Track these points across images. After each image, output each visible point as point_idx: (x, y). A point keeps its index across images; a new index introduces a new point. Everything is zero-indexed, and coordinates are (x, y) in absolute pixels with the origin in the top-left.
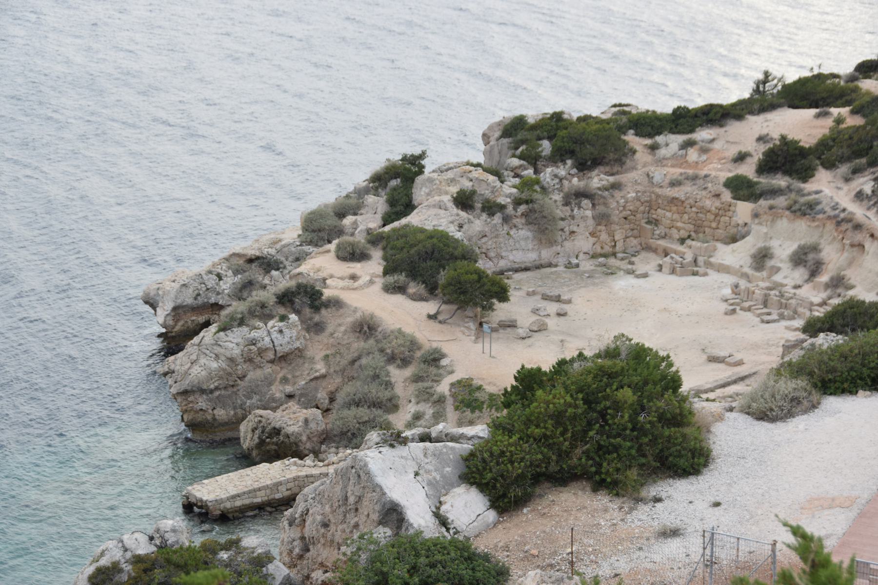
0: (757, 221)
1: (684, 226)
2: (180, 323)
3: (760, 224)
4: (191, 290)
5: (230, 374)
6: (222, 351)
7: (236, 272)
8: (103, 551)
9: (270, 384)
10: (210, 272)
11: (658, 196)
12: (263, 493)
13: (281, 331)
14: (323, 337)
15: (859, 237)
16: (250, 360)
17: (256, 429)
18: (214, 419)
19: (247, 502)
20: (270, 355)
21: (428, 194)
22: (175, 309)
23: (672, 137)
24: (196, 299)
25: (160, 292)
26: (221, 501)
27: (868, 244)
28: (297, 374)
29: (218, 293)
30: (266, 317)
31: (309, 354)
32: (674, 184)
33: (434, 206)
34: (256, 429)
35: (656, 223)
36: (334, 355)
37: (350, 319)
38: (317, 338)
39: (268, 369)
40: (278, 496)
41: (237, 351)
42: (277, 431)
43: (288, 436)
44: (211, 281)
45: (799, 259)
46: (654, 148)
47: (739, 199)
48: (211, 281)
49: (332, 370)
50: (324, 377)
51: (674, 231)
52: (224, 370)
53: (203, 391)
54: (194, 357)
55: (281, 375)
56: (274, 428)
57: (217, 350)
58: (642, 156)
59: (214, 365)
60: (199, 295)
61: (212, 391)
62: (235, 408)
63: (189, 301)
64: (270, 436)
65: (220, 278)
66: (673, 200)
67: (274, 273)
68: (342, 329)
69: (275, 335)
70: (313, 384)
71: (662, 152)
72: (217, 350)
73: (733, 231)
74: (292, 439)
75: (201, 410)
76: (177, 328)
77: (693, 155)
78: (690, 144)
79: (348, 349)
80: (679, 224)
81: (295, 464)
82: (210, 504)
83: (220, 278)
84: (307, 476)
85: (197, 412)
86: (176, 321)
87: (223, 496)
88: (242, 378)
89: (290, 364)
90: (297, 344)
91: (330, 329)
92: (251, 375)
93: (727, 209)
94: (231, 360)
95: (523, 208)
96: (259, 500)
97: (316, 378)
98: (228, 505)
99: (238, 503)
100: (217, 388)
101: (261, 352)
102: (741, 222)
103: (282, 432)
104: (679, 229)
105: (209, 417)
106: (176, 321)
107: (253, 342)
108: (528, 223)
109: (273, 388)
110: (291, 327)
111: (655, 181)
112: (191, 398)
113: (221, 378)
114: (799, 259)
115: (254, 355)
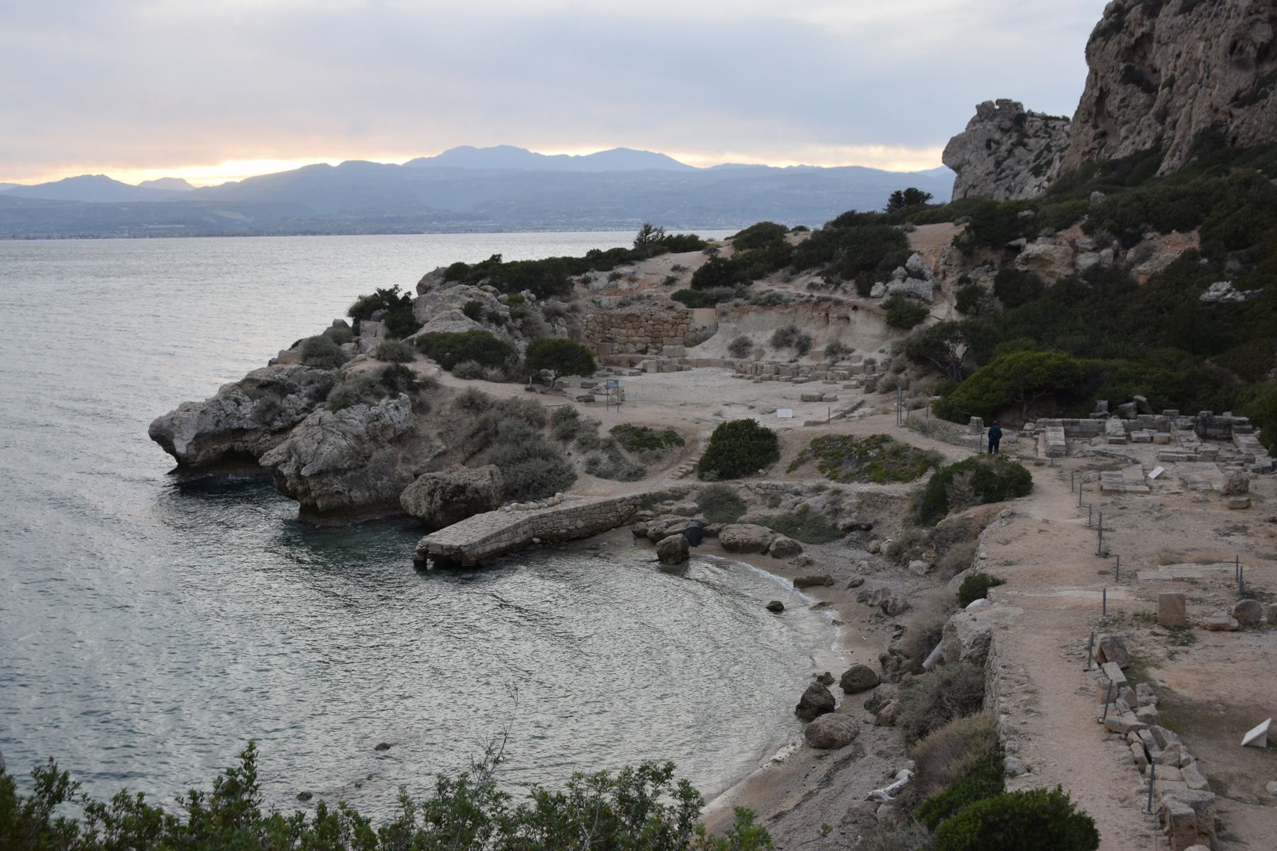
0: (724, 319)
1: (640, 339)
2: (202, 453)
3: (727, 321)
4: (210, 417)
5: (358, 453)
6: (348, 428)
7: (253, 398)
8: (681, 477)
9: (393, 465)
10: (226, 398)
11: (611, 316)
12: (505, 537)
13: (397, 408)
14: (431, 416)
15: (843, 311)
16: (374, 438)
17: (434, 491)
18: (351, 502)
19: (495, 546)
20: (390, 434)
21: (433, 311)
22: (197, 437)
23: (597, 273)
24: (217, 425)
25: (176, 422)
26: (472, 546)
27: (852, 315)
28: (417, 452)
29: (239, 419)
30: (380, 396)
31: (422, 433)
32: (622, 305)
33: (447, 318)
34: (434, 491)
35: (611, 340)
36: (448, 432)
37: (452, 398)
38: (425, 417)
39: (389, 449)
40: (518, 540)
41: (362, 429)
42: (461, 489)
43: (477, 491)
44: (230, 407)
45: (782, 340)
46: (586, 282)
47: (695, 307)
48: (230, 407)
49: (450, 447)
50: (444, 453)
51: (630, 346)
52: (353, 448)
53: (337, 471)
54: (319, 436)
55: (400, 456)
56: (458, 486)
57: (343, 427)
58: (578, 288)
59: (344, 443)
60: (219, 421)
61: (346, 471)
62: (369, 489)
63: (211, 428)
64: (454, 495)
65: (239, 404)
66: (629, 318)
67: (290, 396)
68: (448, 407)
69: (392, 412)
70: (436, 460)
71: (595, 284)
72: (343, 427)
73: (692, 336)
74: (483, 494)
75: (338, 492)
76: (199, 458)
77: (623, 285)
78: (616, 277)
79: (459, 425)
80: (635, 338)
81: (518, 508)
82: (464, 549)
83: (239, 404)
84: (541, 517)
85: (332, 495)
86: (199, 450)
87: (476, 540)
88: (368, 458)
89: (404, 445)
90: (411, 424)
91: (435, 408)
92: (375, 456)
93: (684, 317)
94: (358, 437)
95: (519, 321)
96: (503, 545)
97: (439, 455)
98: (480, 550)
99: (488, 548)
100: (349, 469)
101: (385, 427)
102: (699, 327)
103: (470, 488)
104: (634, 343)
105: (346, 500)
106: (199, 450)
107: (378, 417)
108: (525, 336)
109: (397, 467)
110: (404, 404)
111: (603, 304)
112: (325, 481)
113: (351, 457)
114: (782, 340)
115: (377, 433)
